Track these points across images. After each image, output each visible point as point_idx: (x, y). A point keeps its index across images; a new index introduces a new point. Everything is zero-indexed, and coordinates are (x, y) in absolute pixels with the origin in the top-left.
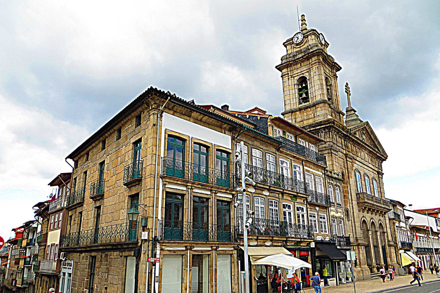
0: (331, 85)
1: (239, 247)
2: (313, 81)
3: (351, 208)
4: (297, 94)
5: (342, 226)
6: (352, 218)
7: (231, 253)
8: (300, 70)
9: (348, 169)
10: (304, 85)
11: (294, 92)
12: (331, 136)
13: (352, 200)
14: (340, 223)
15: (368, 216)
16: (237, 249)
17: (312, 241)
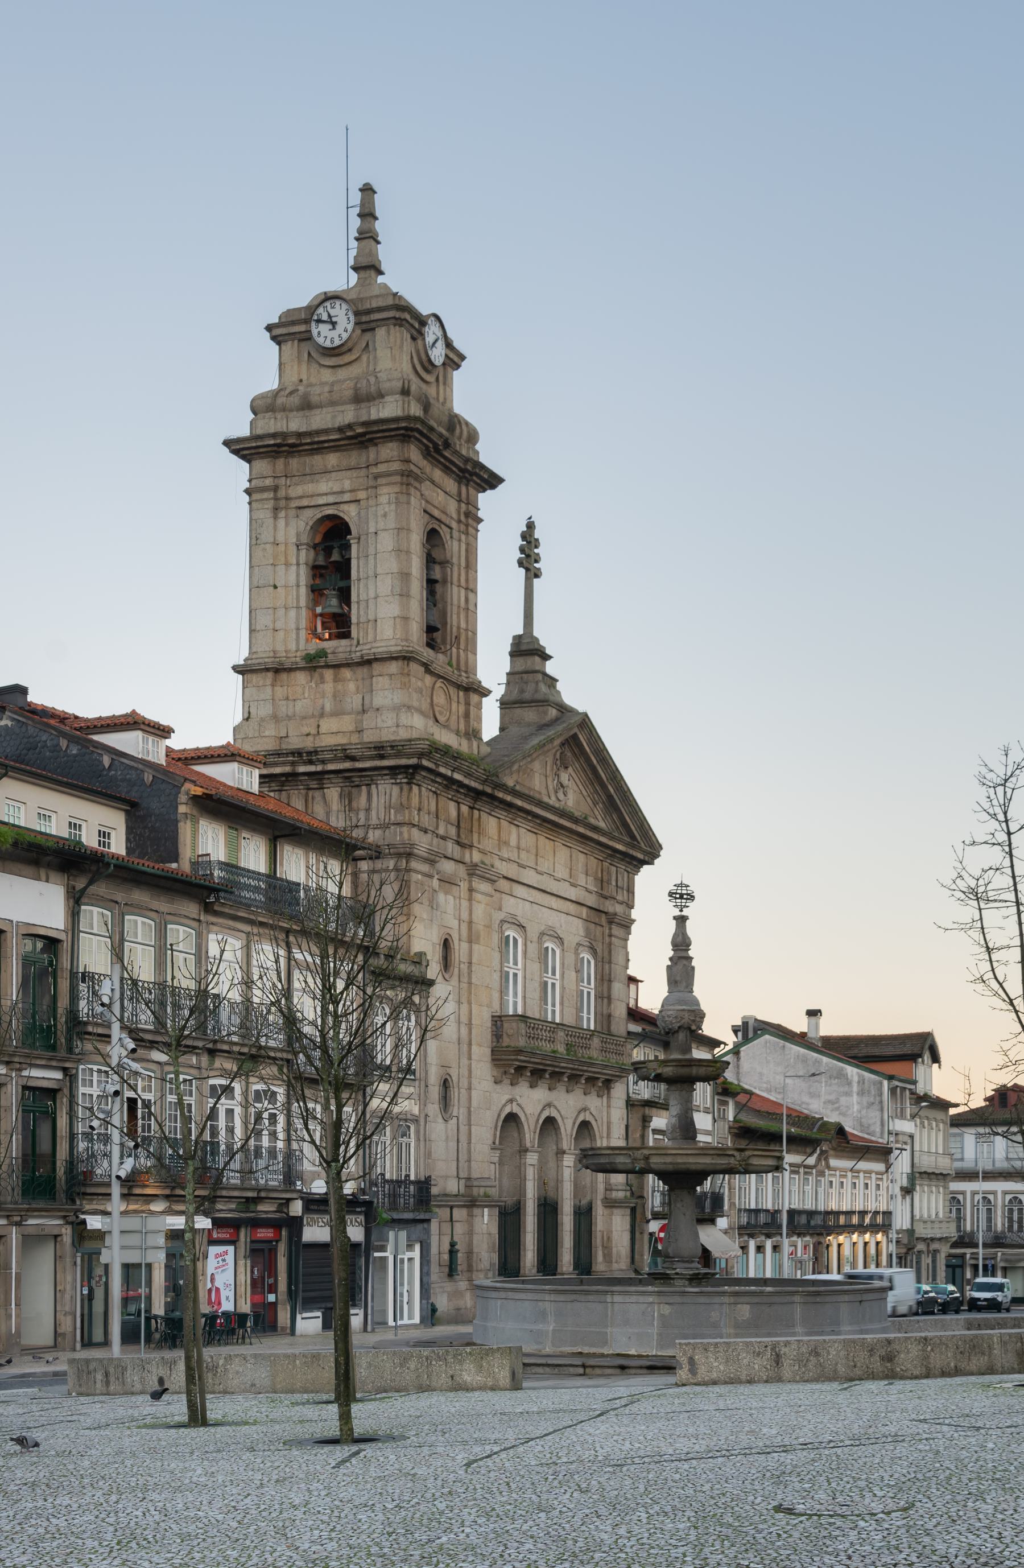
0: (444, 563)
1: (77, 1217)
2: (371, 550)
3: (464, 1071)
4: (303, 590)
5: (408, 1145)
6: (463, 1111)
7: (56, 1232)
8: (329, 485)
9: (470, 922)
10: (335, 557)
11: (294, 578)
12: (415, 801)
13: (470, 1044)
14: (404, 1135)
15: (532, 1100)
16: (72, 1223)
17: (294, 1195)
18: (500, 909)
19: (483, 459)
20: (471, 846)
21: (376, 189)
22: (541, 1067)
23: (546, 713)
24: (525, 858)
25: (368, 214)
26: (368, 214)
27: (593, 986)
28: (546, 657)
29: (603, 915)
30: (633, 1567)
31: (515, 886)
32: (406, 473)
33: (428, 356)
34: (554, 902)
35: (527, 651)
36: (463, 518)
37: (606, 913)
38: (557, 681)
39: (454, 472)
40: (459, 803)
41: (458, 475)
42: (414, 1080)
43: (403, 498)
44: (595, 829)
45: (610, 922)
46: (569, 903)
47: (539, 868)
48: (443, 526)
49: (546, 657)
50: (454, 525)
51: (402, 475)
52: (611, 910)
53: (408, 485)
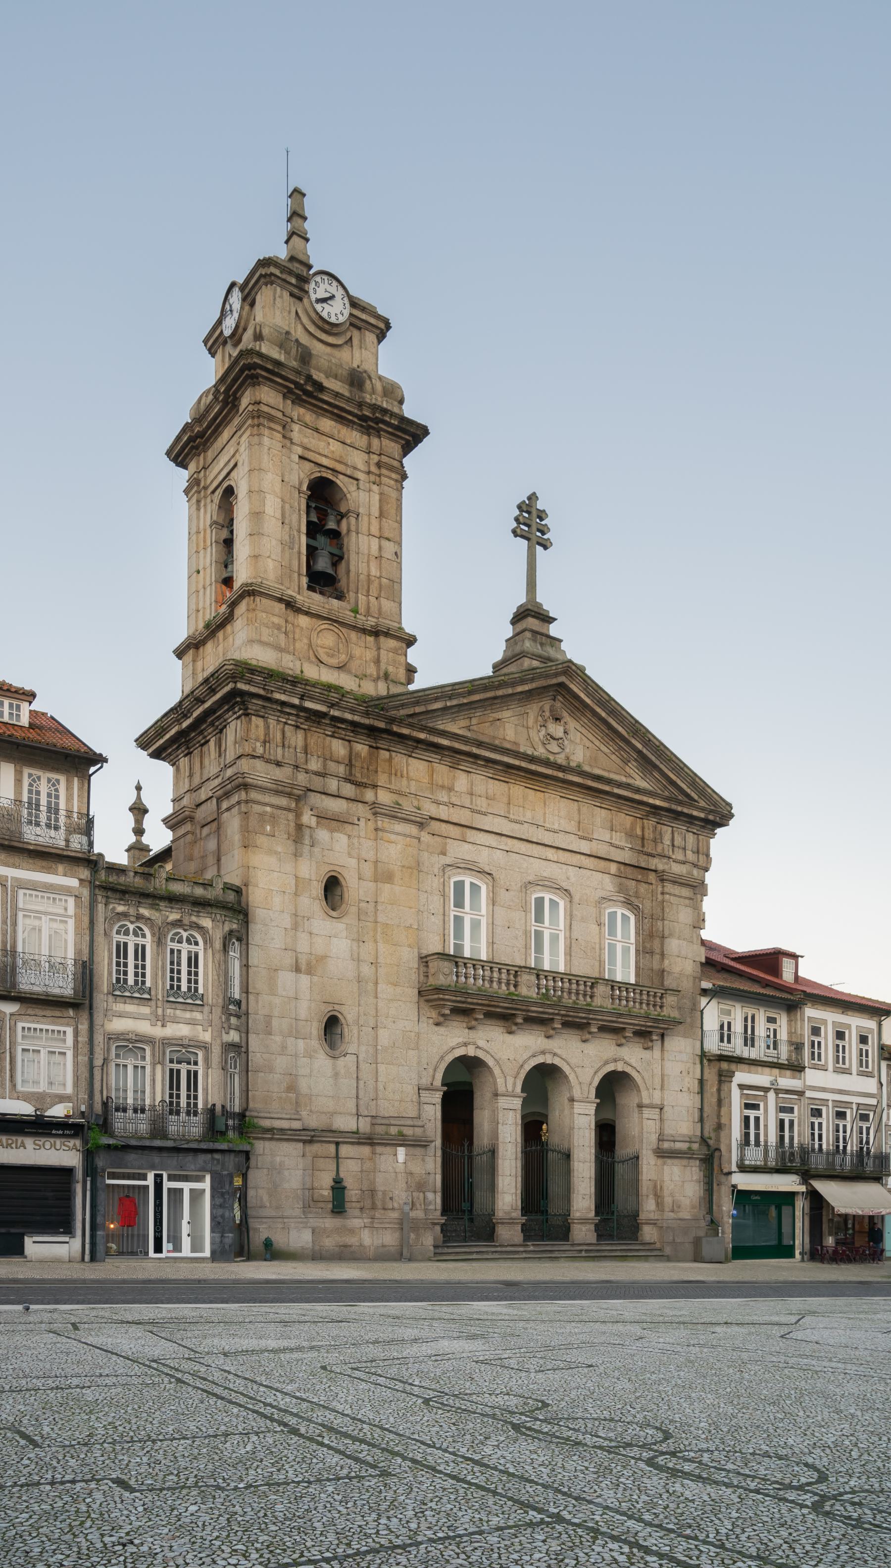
18: (444, 854)
19: (406, 415)
20: (375, 786)
21: (304, 191)
22: (622, 1026)
23: (522, 665)
24: (481, 804)
25: (296, 215)
26: (296, 215)
27: (633, 940)
28: (549, 620)
29: (653, 874)
30: (382, 1566)
31: (468, 831)
32: (255, 414)
33: (321, 318)
34: (550, 854)
35: (531, 616)
36: (373, 469)
37: (655, 871)
38: (560, 641)
39: (354, 423)
40: (349, 741)
41: (362, 426)
42: (150, 999)
43: (256, 439)
44: (638, 790)
45: (662, 880)
46: (583, 857)
47: (511, 816)
48: (341, 477)
49: (549, 620)
50: (361, 476)
51: (253, 418)
52: (660, 867)
53: (258, 426)
